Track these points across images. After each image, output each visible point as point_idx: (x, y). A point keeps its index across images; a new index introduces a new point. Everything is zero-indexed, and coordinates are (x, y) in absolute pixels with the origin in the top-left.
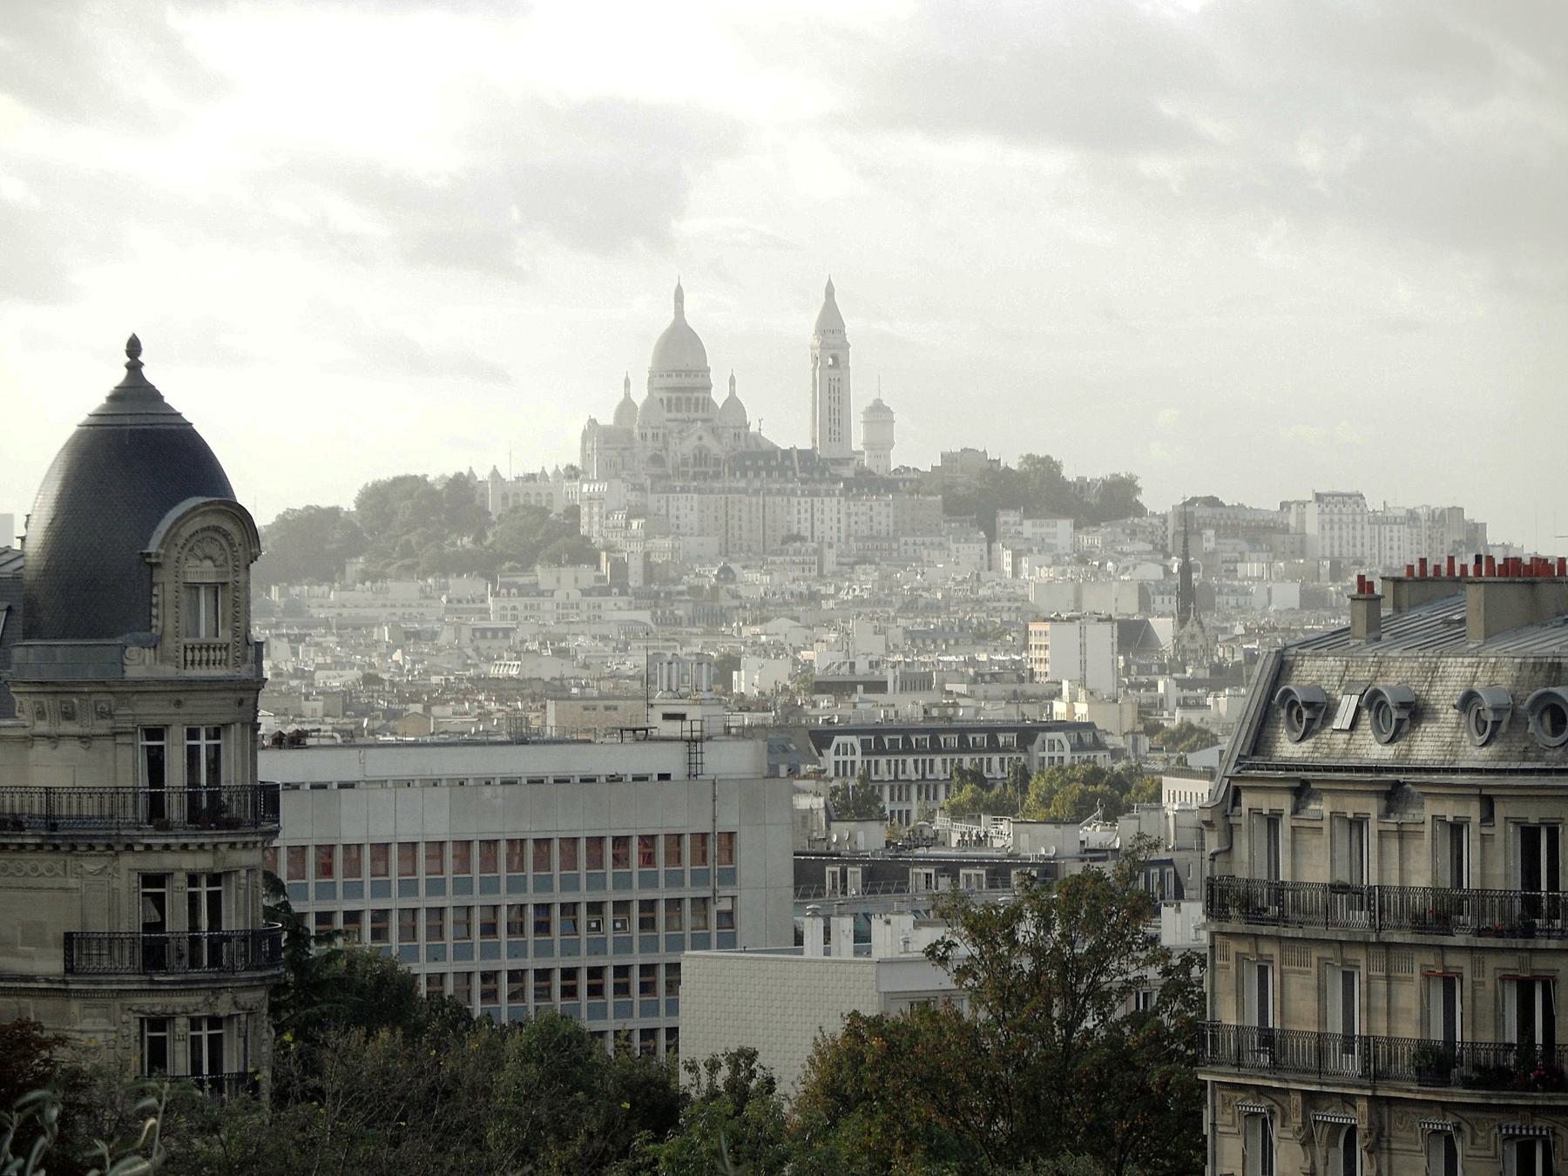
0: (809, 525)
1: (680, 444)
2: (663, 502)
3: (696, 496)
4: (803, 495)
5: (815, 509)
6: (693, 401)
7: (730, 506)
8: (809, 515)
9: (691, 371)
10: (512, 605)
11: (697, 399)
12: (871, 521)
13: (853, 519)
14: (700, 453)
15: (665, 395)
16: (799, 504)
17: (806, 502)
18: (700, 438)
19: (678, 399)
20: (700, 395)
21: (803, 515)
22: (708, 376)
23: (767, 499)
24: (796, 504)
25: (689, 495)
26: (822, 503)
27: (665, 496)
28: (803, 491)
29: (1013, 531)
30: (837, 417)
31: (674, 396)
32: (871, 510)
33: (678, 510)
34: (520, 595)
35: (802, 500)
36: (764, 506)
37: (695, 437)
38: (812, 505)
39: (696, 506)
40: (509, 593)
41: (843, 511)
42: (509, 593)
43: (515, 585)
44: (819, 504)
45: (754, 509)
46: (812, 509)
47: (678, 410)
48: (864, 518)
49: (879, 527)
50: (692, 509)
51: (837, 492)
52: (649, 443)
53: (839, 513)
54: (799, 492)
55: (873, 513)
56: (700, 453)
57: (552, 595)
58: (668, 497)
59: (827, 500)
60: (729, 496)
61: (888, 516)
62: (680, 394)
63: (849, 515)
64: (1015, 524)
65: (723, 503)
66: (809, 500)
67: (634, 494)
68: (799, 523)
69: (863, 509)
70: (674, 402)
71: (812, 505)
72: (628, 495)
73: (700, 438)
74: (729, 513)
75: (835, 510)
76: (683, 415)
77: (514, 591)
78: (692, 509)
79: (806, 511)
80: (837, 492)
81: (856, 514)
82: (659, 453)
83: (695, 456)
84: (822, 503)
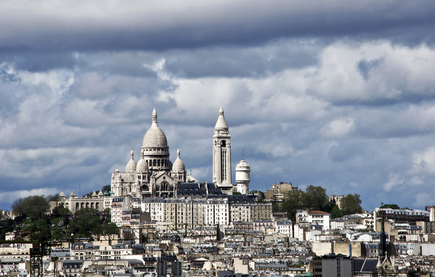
0: (213, 216)
2: (148, 206)
3: (162, 204)
4: (210, 203)
5: (215, 210)
7: (177, 209)
10: (81, 252)
12: (240, 215)
13: (232, 214)
14: (164, 184)
15: (148, 159)
17: (211, 206)
18: (164, 178)
19: (155, 160)
20: (165, 159)
21: (210, 212)
22: (168, 150)
24: (207, 207)
25: (160, 203)
26: (219, 207)
28: (210, 201)
31: (153, 159)
32: (240, 210)
35: (210, 205)
38: (214, 207)
39: (162, 208)
40: (79, 247)
42: (79, 247)
45: (188, 209)
46: (214, 209)
48: (237, 213)
49: (244, 218)
50: (161, 210)
52: (141, 180)
56: (164, 184)
58: (150, 204)
59: (220, 205)
61: (248, 213)
62: (155, 158)
63: (230, 212)
65: (174, 206)
66: (213, 205)
70: (153, 161)
71: (214, 207)
73: (164, 178)
77: (82, 246)
78: (161, 210)
79: (211, 210)
82: (146, 184)
83: (162, 186)
84: (219, 207)
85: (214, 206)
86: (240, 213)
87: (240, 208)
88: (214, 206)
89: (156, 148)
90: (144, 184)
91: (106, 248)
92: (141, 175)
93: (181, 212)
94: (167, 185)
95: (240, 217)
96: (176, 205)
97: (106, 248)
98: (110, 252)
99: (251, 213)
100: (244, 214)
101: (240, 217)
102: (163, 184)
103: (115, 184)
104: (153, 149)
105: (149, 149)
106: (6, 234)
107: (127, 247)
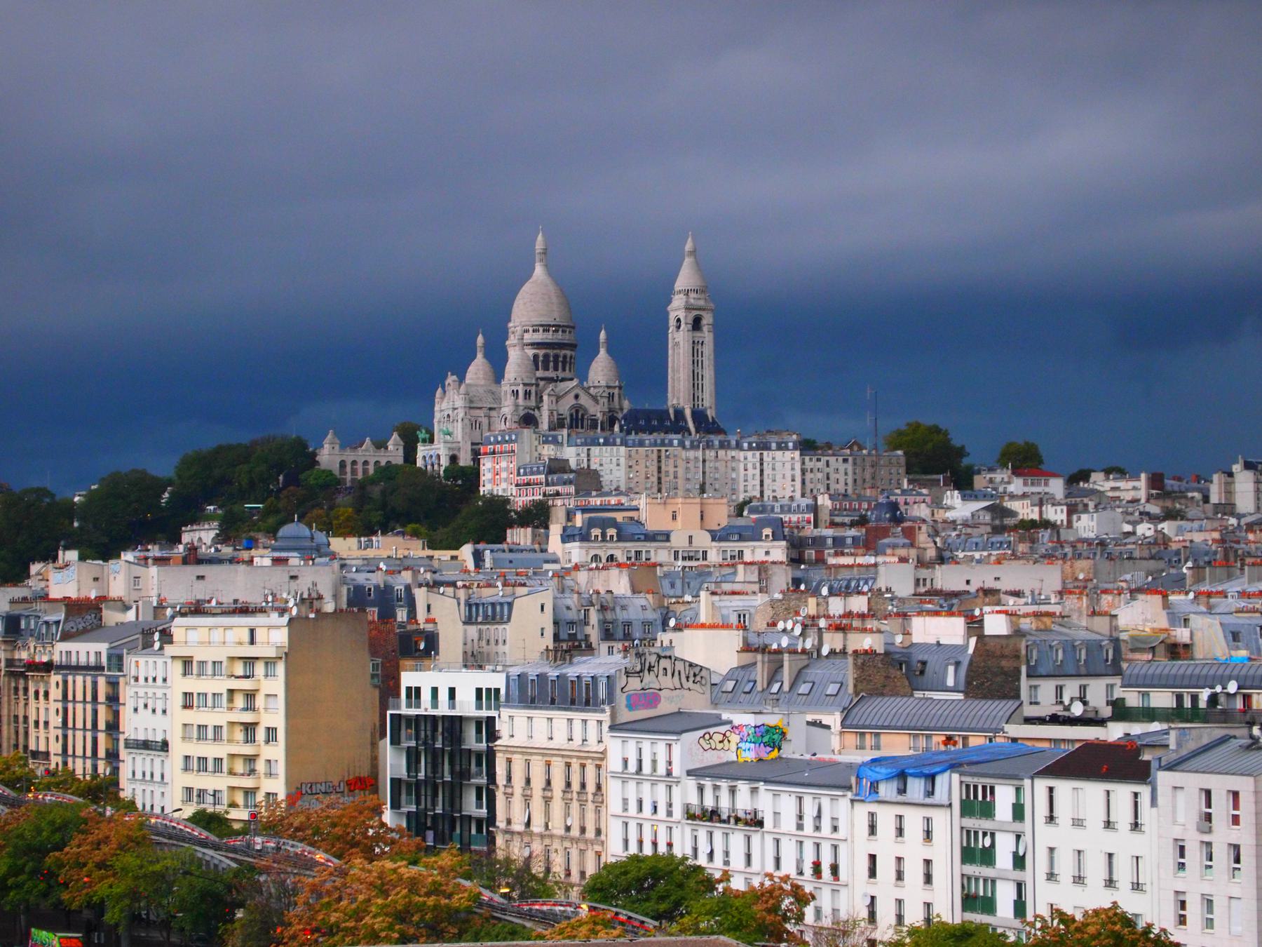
1: (557, 402)
2: (584, 456)
3: (623, 449)
4: (750, 448)
5: (765, 464)
6: (561, 359)
7: (663, 461)
8: (758, 472)
9: (559, 326)
10: (610, 552)
11: (565, 357)
12: (828, 479)
13: (809, 476)
14: (577, 412)
15: (530, 352)
16: (746, 458)
18: (577, 397)
19: (546, 356)
21: (751, 472)
23: (707, 452)
24: (742, 459)
26: (773, 458)
27: (586, 448)
28: (750, 444)
29: (1001, 489)
30: (700, 382)
32: (828, 466)
33: (601, 465)
34: (621, 538)
35: (749, 454)
36: (704, 461)
37: (572, 394)
38: (762, 460)
39: (622, 461)
40: (604, 535)
41: (798, 466)
42: (604, 535)
43: (613, 524)
44: (770, 459)
46: (762, 464)
47: (546, 368)
48: (820, 475)
49: (838, 486)
51: (791, 445)
53: (793, 469)
54: (746, 445)
55: (831, 470)
56: (577, 412)
57: (668, 540)
58: (589, 450)
59: (779, 454)
60: (663, 449)
61: (846, 474)
62: (548, 351)
63: (803, 472)
64: (1002, 481)
65: (655, 456)
66: (758, 453)
67: (546, 446)
68: (746, 481)
69: (821, 465)
70: (541, 358)
71: (762, 460)
72: (540, 448)
73: (577, 397)
74: (663, 468)
75: (788, 466)
76: (551, 374)
77: (612, 532)
78: (618, 465)
80: (791, 445)
81: (812, 470)
82: (532, 412)
83: (571, 415)
85: (761, 454)
86: (828, 474)
87: (828, 462)
88: (761, 454)
89: (550, 326)
90: (526, 411)
91: (691, 537)
92: (521, 389)
93: (671, 470)
94: (583, 415)
95: (828, 485)
96: (659, 451)
97: (691, 537)
98: (705, 553)
99: (855, 473)
100: (837, 476)
101: (828, 485)
102: (573, 411)
103: (450, 413)
104: (541, 329)
105: (531, 329)
106: (183, 528)
107: (767, 536)
